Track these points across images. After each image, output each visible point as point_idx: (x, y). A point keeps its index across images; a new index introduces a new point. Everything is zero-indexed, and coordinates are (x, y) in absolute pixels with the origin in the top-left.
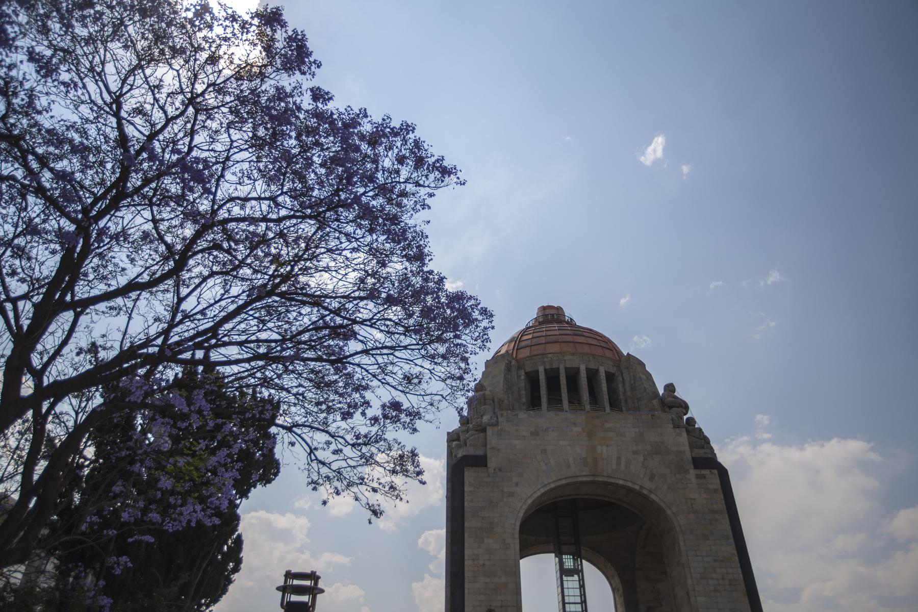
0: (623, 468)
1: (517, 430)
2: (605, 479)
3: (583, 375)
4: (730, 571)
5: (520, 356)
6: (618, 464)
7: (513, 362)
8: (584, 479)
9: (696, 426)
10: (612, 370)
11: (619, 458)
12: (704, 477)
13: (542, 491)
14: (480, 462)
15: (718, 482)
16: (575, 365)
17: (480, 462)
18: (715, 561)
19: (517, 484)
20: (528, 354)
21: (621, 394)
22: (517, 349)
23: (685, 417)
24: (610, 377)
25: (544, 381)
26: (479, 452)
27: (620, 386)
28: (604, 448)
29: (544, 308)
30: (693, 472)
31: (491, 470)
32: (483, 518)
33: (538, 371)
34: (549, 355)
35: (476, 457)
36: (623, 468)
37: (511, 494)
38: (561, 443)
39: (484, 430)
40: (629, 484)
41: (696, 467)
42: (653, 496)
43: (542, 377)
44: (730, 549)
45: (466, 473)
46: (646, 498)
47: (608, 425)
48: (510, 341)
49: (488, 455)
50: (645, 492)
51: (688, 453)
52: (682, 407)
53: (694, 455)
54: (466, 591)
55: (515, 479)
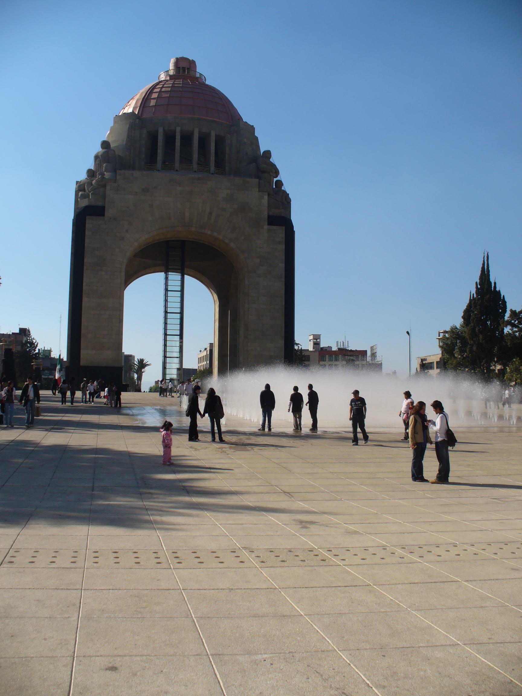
9: (283, 189)
11: (210, 213)
15: (284, 235)
19: (127, 231)
21: (227, 155)
23: (275, 179)
24: (220, 141)
25: (161, 141)
26: (100, 204)
27: (227, 148)
30: (266, 227)
33: (157, 131)
39: (105, 186)
40: (215, 234)
42: (232, 245)
45: (87, 221)
49: (106, 206)
50: (227, 241)
51: (266, 213)
53: (271, 213)
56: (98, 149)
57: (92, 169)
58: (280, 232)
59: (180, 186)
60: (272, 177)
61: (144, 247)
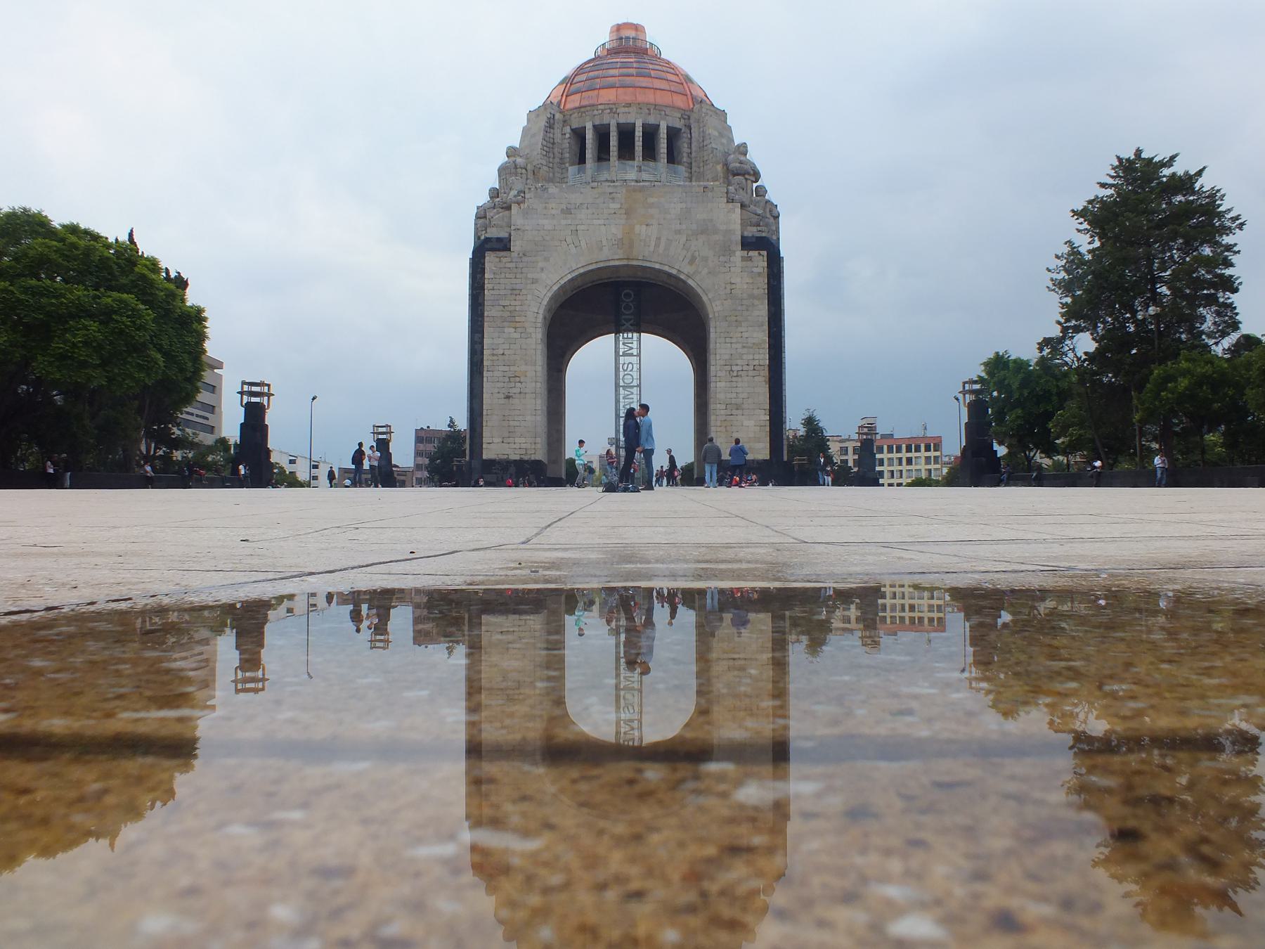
0: (661, 249)
1: (546, 208)
2: (640, 263)
3: (639, 133)
4: (757, 357)
5: (569, 106)
6: (657, 245)
7: (558, 116)
8: (617, 263)
10: (678, 124)
11: (659, 239)
12: (750, 259)
13: (570, 277)
14: (503, 245)
16: (630, 120)
17: (503, 245)
18: (744, 347)
19: (542, 269)
20: (577, 105)
21: (685, 155)
22: (566, 96)
23: (755, 185)
24: (673, 134)
26: (503, 234)
28: (645, 226)
29: (619, 28)
30: (739, 253)
31: (514, 255)
32: (504, 306)
34: (600, 107)
35: (499, 240)
36: (661, 249)
37: (535, 281)
38: (596, 222)
39: (509, 208)
40: (666, 268)
41: (742, 250)
42: (690, 282)
43: (589, 135)
44: (762, 336)
46: (684, 282)
47: (651, 200)
48: (561, 83)
50: (682, 277)
51: (739, 233)
52: (749, 174)
53: (746, 234)
54: (485, 379)
55: (540, 264)
56: (502, 158)
57: (495, 189)
58: (760, 260)
59: (614, 202)
60: (749, 182)
61: (574, 292)
